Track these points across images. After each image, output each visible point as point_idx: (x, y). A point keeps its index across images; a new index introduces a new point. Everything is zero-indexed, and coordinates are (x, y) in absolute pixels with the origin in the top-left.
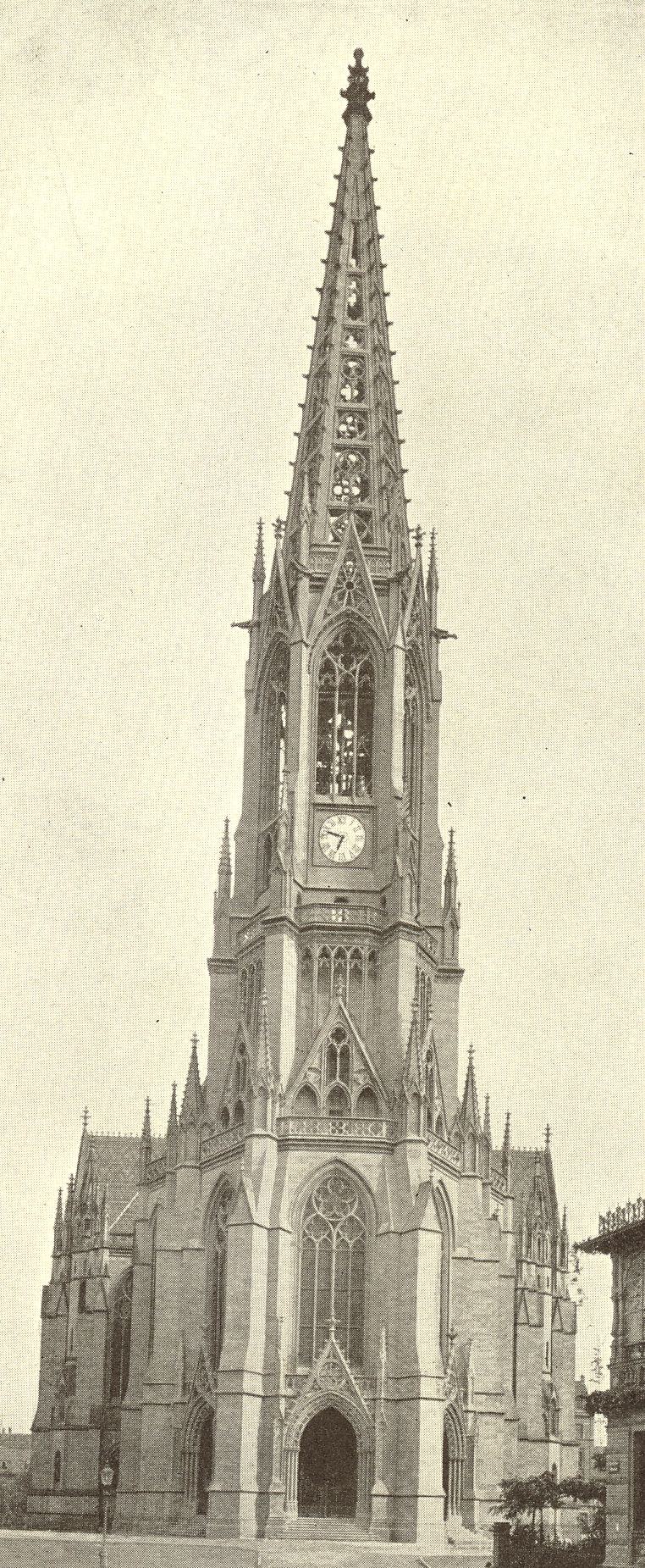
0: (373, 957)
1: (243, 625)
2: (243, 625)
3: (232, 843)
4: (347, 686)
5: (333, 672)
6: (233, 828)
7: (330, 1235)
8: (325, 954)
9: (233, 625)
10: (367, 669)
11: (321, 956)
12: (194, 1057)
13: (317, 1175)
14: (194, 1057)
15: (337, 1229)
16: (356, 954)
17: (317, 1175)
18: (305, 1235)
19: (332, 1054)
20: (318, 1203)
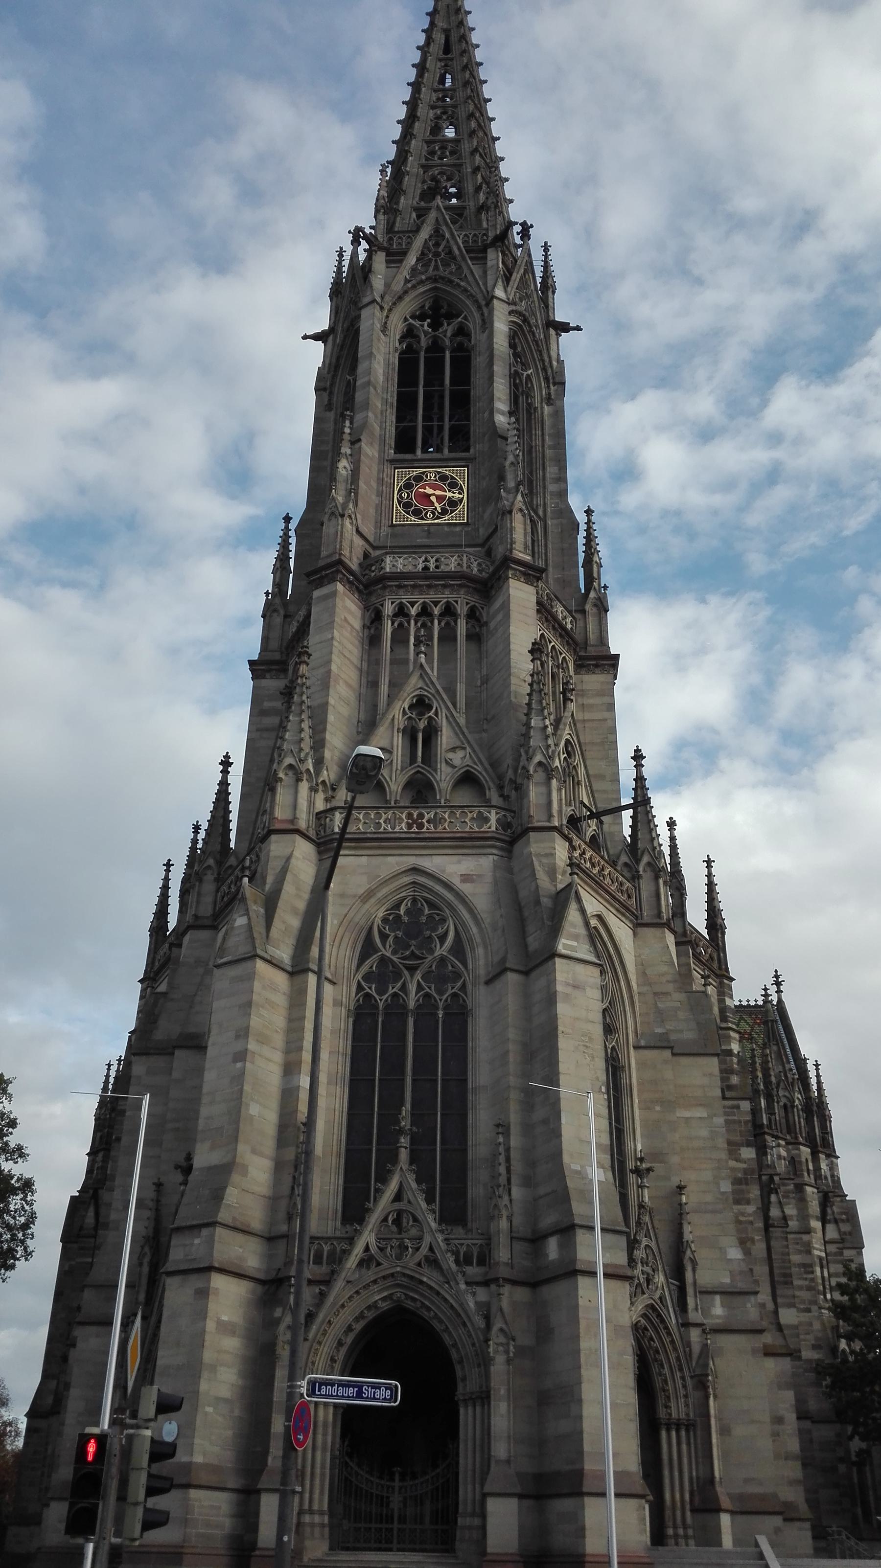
0: (472, 615)
1: (316, 337)
2: (316, 337)
3: (293, 540)
4: (436, 347)
5: (417, 338)
6: (293, 525)
7: (404, 988)
8: (401, 611)
9: (305, 337)
11: (395, 615)
12: (224, 785)
13: (385, 891)
14: (224, 785)
15: (418, 976)
16: (449, 611)
17: (385, 891)
18: (360, 988)
19: (410, 734)
20: (384, 937)
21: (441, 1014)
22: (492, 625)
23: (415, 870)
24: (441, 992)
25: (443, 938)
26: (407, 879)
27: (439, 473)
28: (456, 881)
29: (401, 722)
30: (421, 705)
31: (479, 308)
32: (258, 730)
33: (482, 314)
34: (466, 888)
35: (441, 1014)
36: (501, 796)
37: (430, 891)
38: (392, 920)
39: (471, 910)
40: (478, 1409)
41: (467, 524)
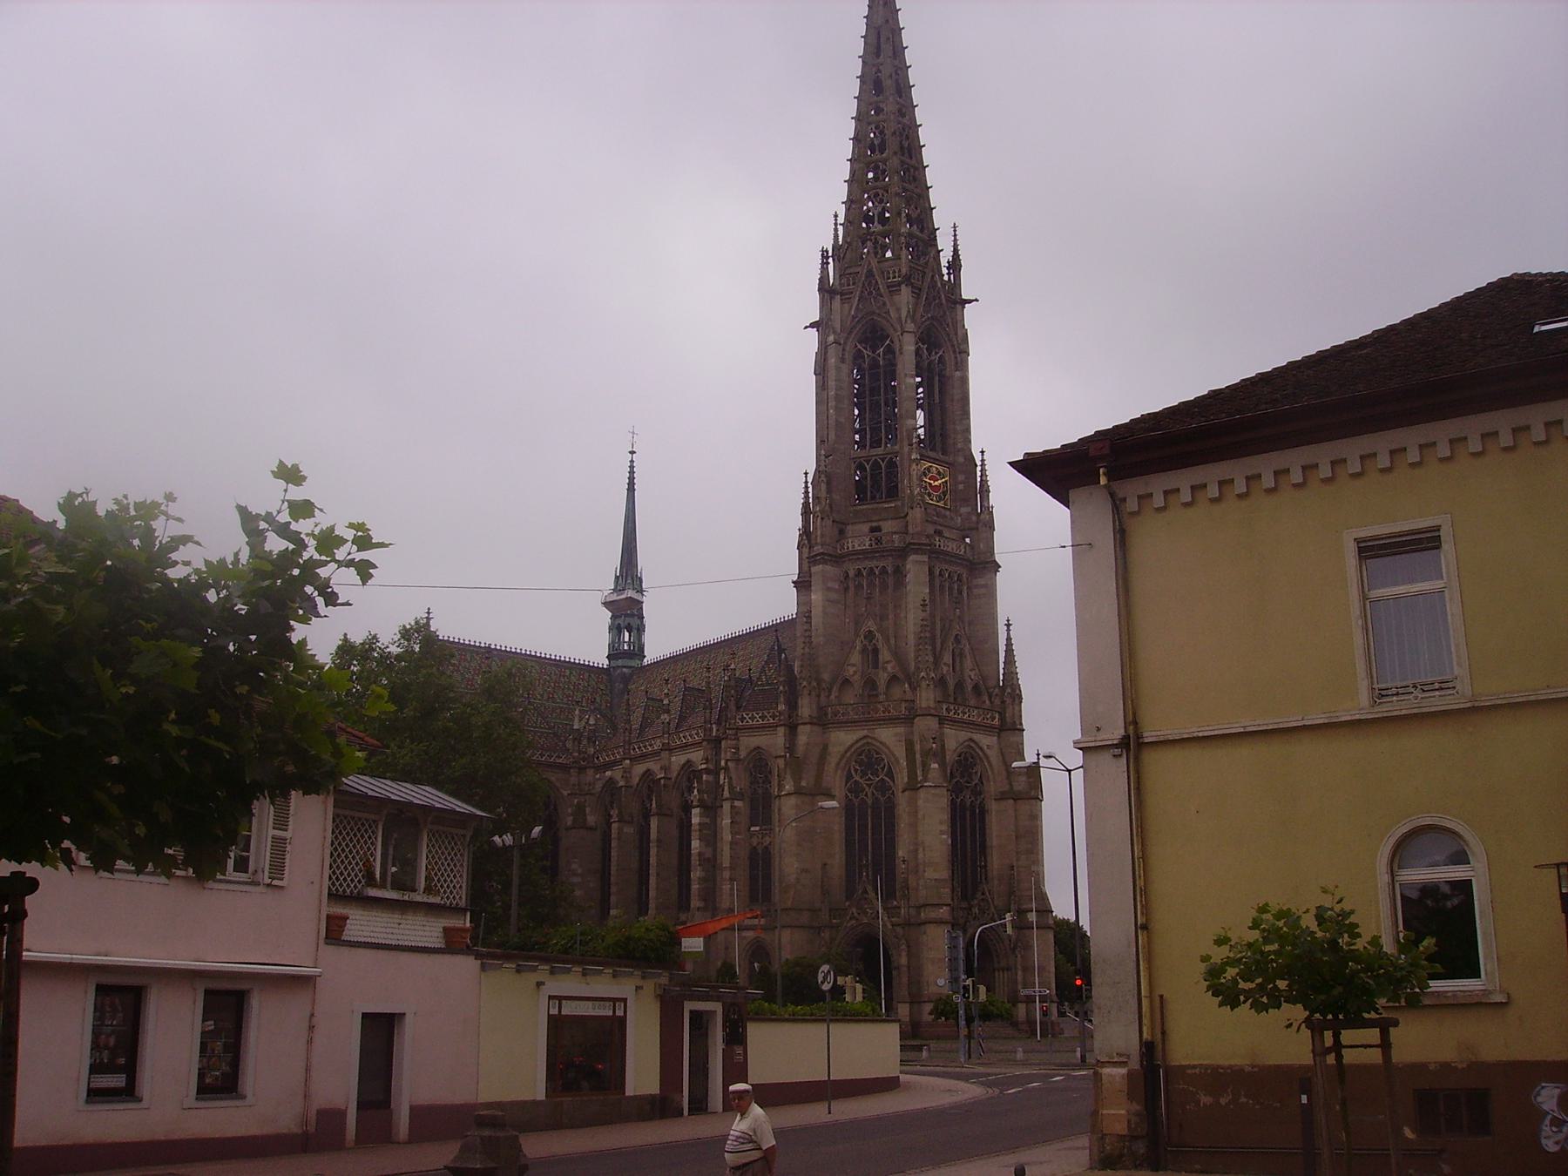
10: (890, 350)
21: (977, 811)
22: (976, 591)
23: (971, 740)
24: (976, 800)
25: (976, 773)
26: (967, 743)
27: (937, 468)
28: (985, 748)
29: (951, 649)
30: (957, 639)
31: (954, 352)
32: (828, 601)
33: (956, 358)
34: (988, 752)
35: (977, 811)
36: (990, 700)
37: (974, 750)
38: (959, 762)
39: (989, 762)
40: (1005, 972)
41: (949, 509)
